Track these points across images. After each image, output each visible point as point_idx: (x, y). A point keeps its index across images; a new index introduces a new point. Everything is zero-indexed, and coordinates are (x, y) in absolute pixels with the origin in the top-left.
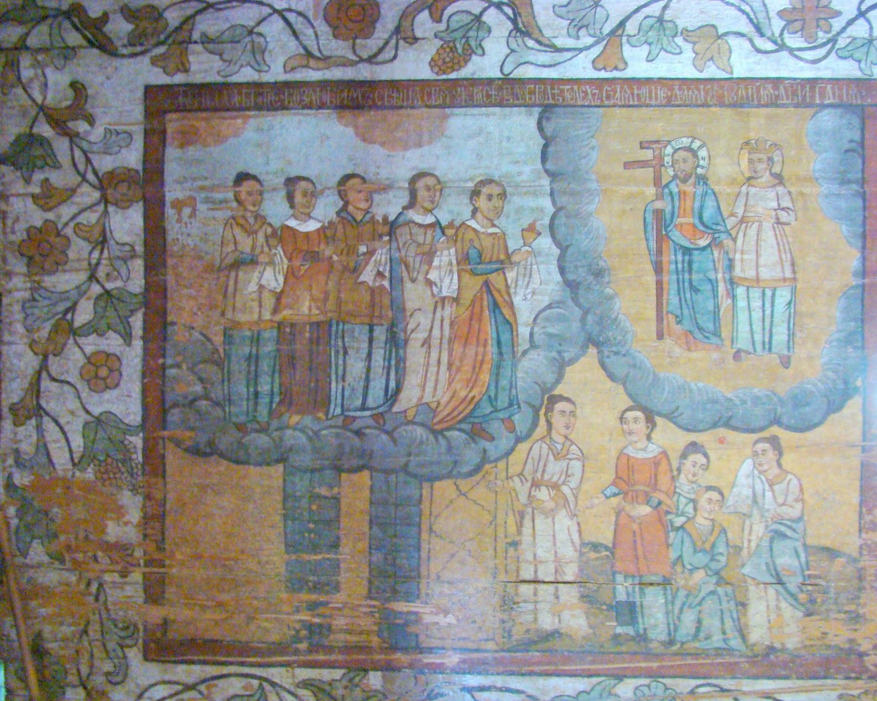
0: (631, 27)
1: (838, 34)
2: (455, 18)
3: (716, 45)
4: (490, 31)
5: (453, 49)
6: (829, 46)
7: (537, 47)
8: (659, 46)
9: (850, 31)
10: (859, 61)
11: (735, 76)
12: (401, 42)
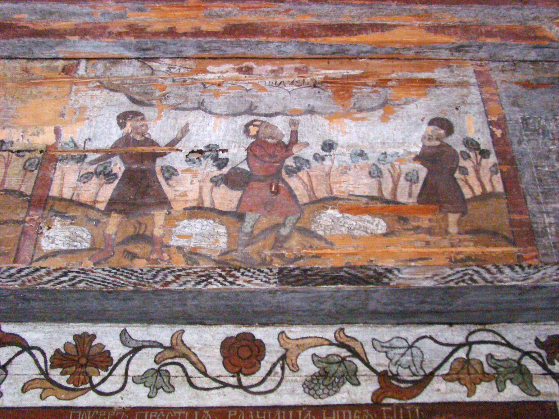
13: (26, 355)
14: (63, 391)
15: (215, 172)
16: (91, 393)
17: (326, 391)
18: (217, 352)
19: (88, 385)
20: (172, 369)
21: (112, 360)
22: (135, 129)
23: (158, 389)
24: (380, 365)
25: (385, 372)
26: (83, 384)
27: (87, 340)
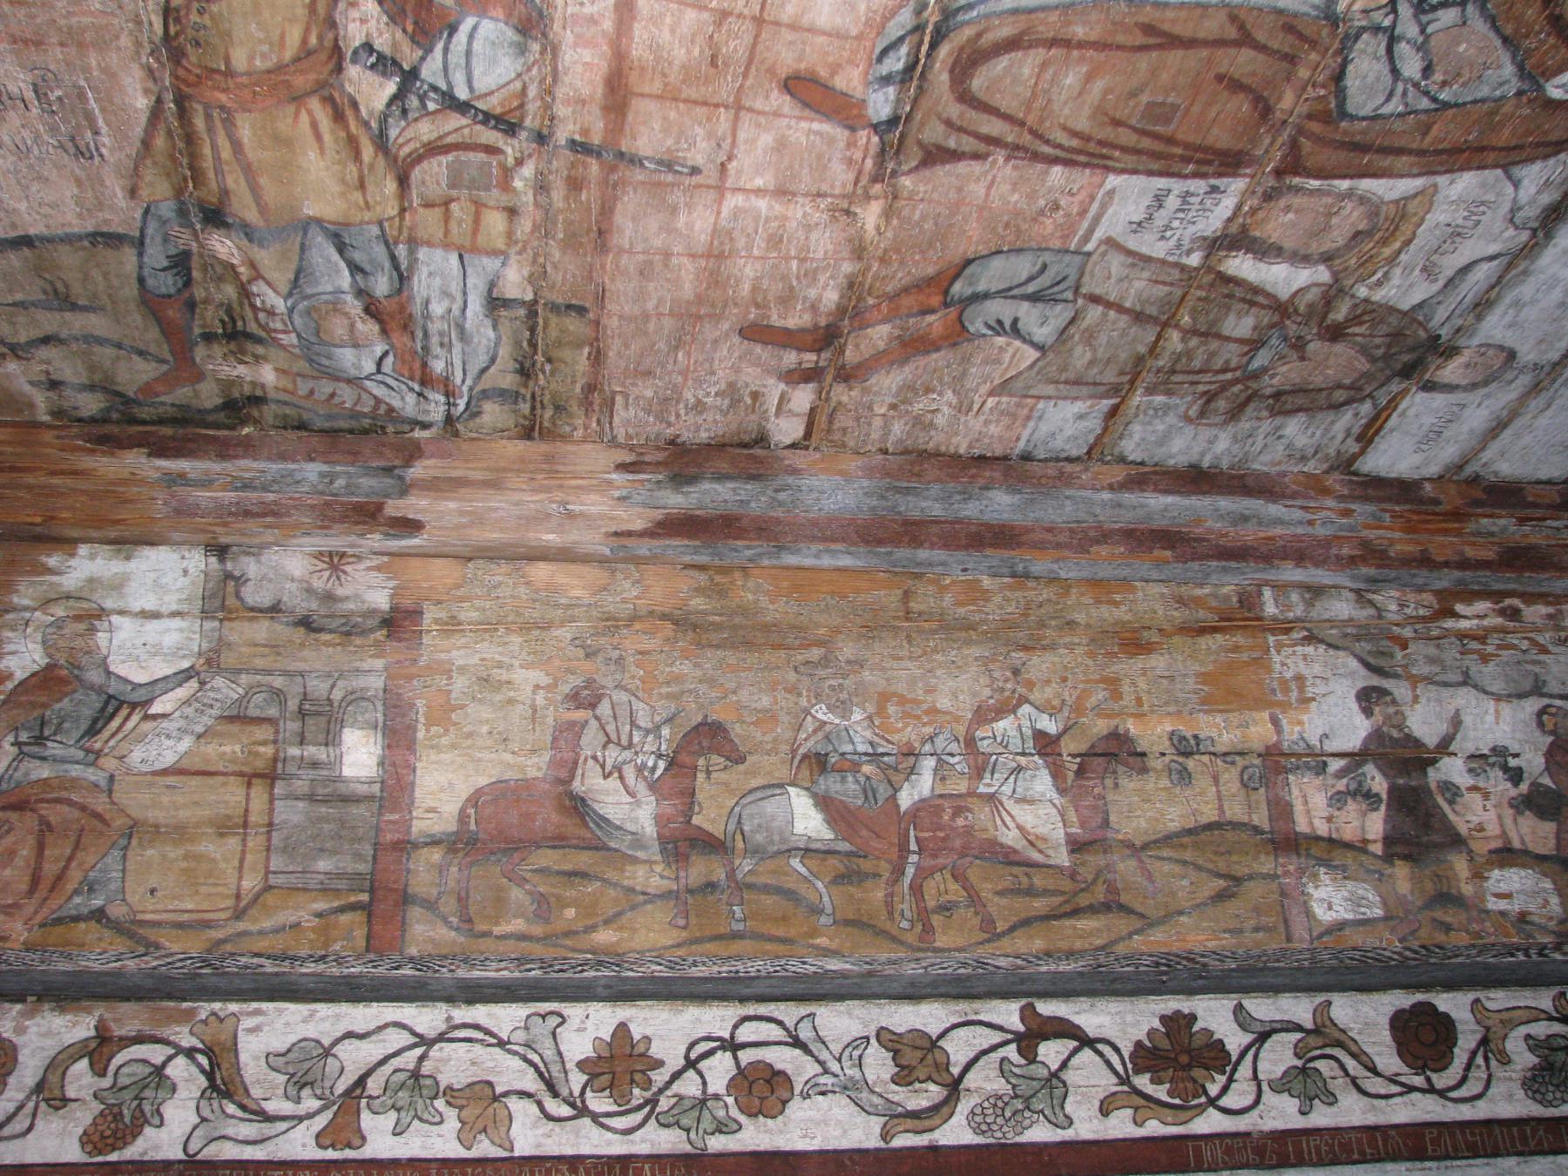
0: (374, 1085)
1: (661, 1091)
2: (125, 1070)
3: (490, 1110)
4: (174, 1089)
5: (117, 1117)
6: (647, 1109)
7: (240, 1113)
8: (412, 1113)
9: (676, 1087)
10: (688, 1130)
11: (516, 1154)
12: (43, 1105)
13: (1087, 1055)
14: (1167, 1111)
15: (1513, 792)
16: (1211, 1109)
17: (1558, 1095)
18: (1386, 1035)
19: (1203, 1099)
20: (1321, 1065)
22: (1388, 718)
23: (1311, 1100)
26: (1194, 1097)
27: (1183, 1022)
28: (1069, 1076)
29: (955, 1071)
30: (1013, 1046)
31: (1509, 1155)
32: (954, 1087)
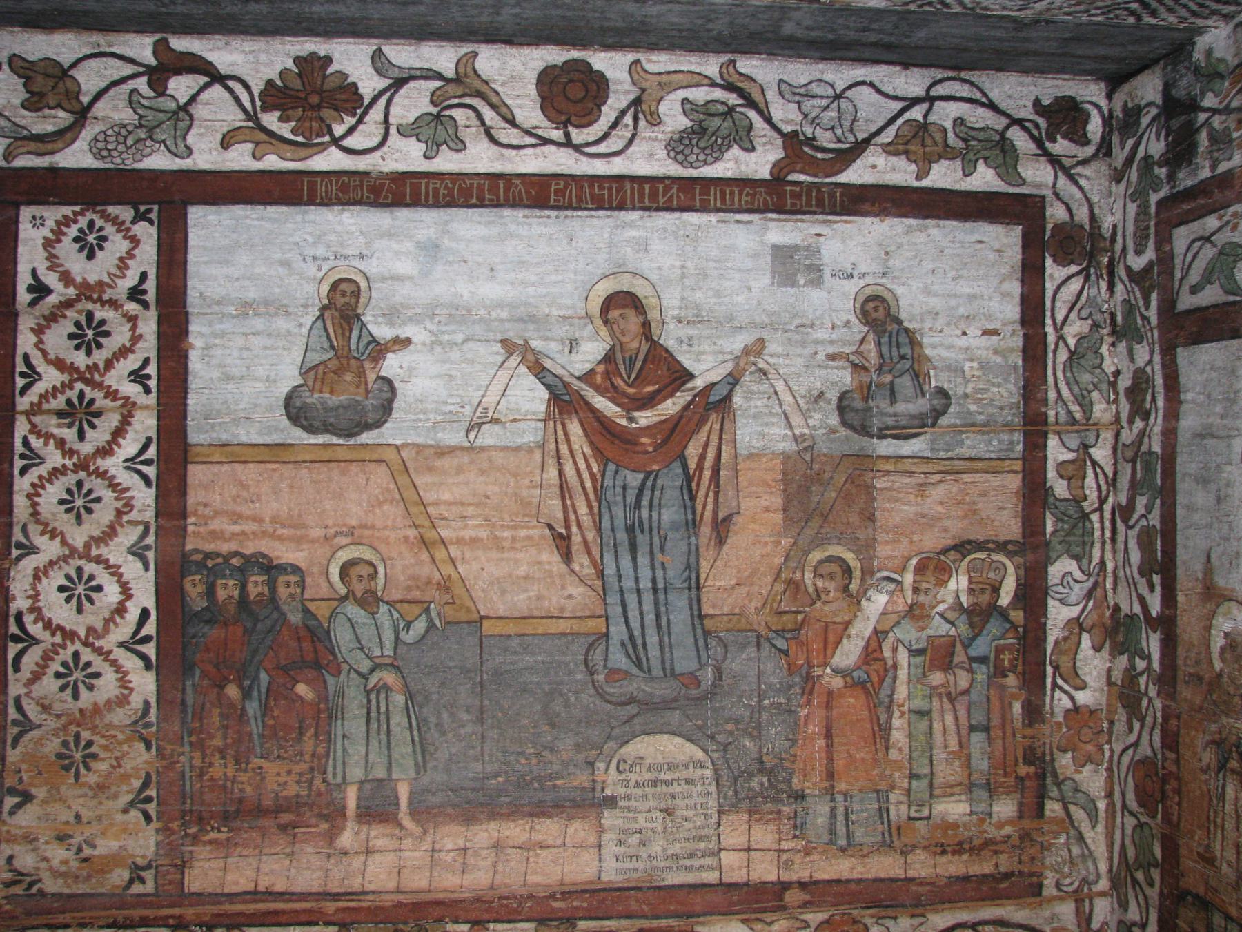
13: (217, 90)
14: (289, 147)
16: (333, 149)
17: (702, 157)
18: (532, 89)
19: (327, 138)
20: (457, 114)
21: (361, 98)
23: (438, 145)
24: (788, 122)
25: (795, 134)
26: (318, 136)
28: (198, 111)
29: (85, 100)
30: (144, 79)
31: (634, 209)
32: (82, 115)
